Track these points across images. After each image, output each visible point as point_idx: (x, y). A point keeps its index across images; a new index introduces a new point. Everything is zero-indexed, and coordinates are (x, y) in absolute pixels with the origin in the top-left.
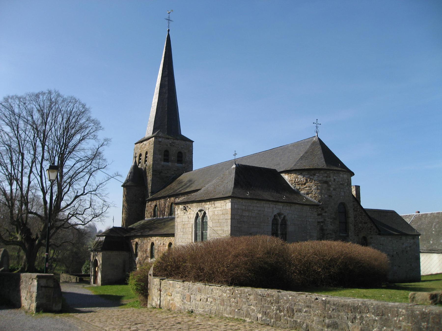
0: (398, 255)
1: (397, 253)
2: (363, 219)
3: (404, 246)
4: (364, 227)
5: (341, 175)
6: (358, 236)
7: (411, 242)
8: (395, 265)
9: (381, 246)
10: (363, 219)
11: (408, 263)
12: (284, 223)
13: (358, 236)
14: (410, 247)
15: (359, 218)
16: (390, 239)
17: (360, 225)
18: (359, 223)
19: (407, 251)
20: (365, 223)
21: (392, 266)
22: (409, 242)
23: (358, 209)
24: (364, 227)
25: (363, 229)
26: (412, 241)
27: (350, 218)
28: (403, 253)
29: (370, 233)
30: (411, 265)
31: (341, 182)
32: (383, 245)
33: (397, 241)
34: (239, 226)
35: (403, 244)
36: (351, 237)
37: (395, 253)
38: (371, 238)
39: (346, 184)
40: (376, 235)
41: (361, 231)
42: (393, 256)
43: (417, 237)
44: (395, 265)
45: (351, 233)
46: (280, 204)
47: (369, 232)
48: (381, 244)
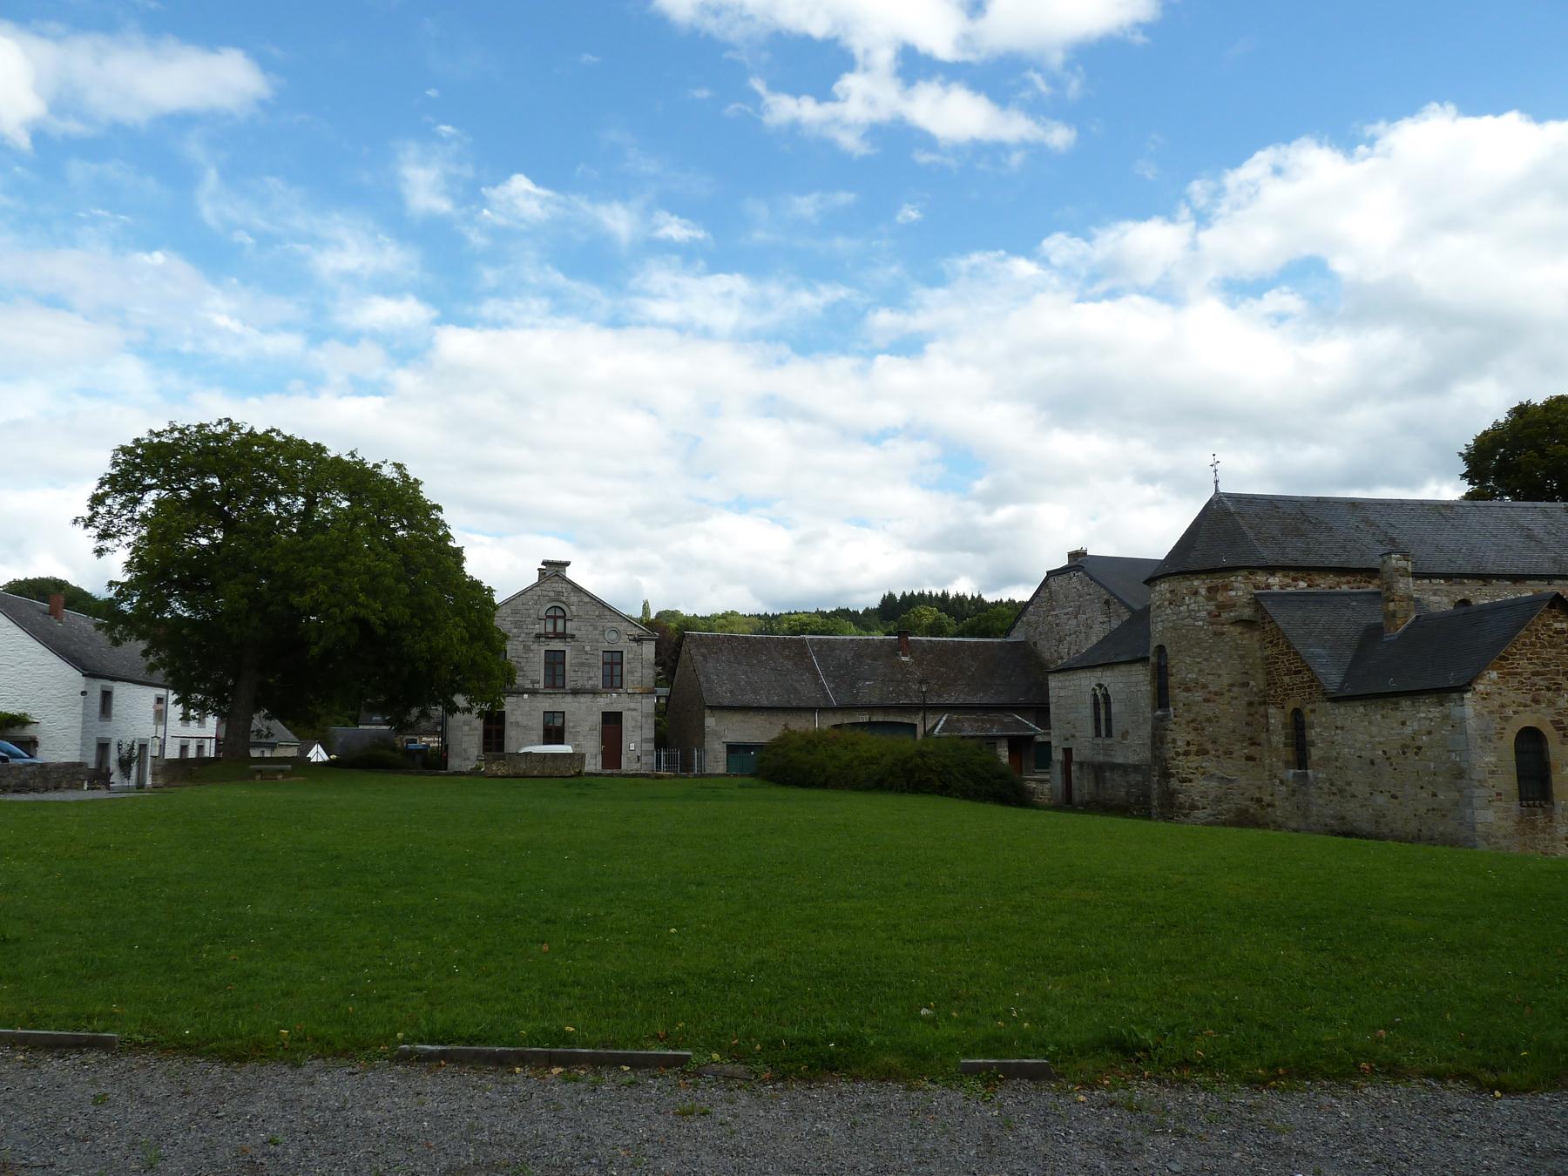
0: (1387, 759)
1: (1385, 752)
2: (1293, 663)
3: (1408, 730)
4: (1295, 684)
5: (1158, 588)
6: (1283, 708)
7: (1430, 716)
8: (1381, 792)
9: (1338, 732)
10: (1293, 663)
11: (1422, 788)
12: (1107, 697)
13: (1283, 708)
14: (1430, 733)
15: (1283, 662)
16: (1361, 709)
17: (1286, 679)
18: (1285, 675)
19: (1419, 748)
20: (1296, 673)
21: (1372, 794)
22: (1423, 715)
23: (1279, 639)
24: (1295, 684)
25: (1292, 689)
26: (1435, 712)
27: (1172, 676)
28: (1404, 753)
29: (1310, 698)
30: (1434, 795)
31: (1158, 603)
32: (1342, 728)
33: (1383, 716)
34: (1058, 712)
35: (1403, 723)
36: (1175, 716)
37: (1380, 753)
38: (1313, 711)
39: (1166, 603)
40: (1323, 701)
41: (1288, 694)
42: (1372, 763)
43: (1455, 696)
44: (1381, 792)
45: (1175, 709)
46: (1099, 669)
47: (1307, 696)
48: (1337, 728)
